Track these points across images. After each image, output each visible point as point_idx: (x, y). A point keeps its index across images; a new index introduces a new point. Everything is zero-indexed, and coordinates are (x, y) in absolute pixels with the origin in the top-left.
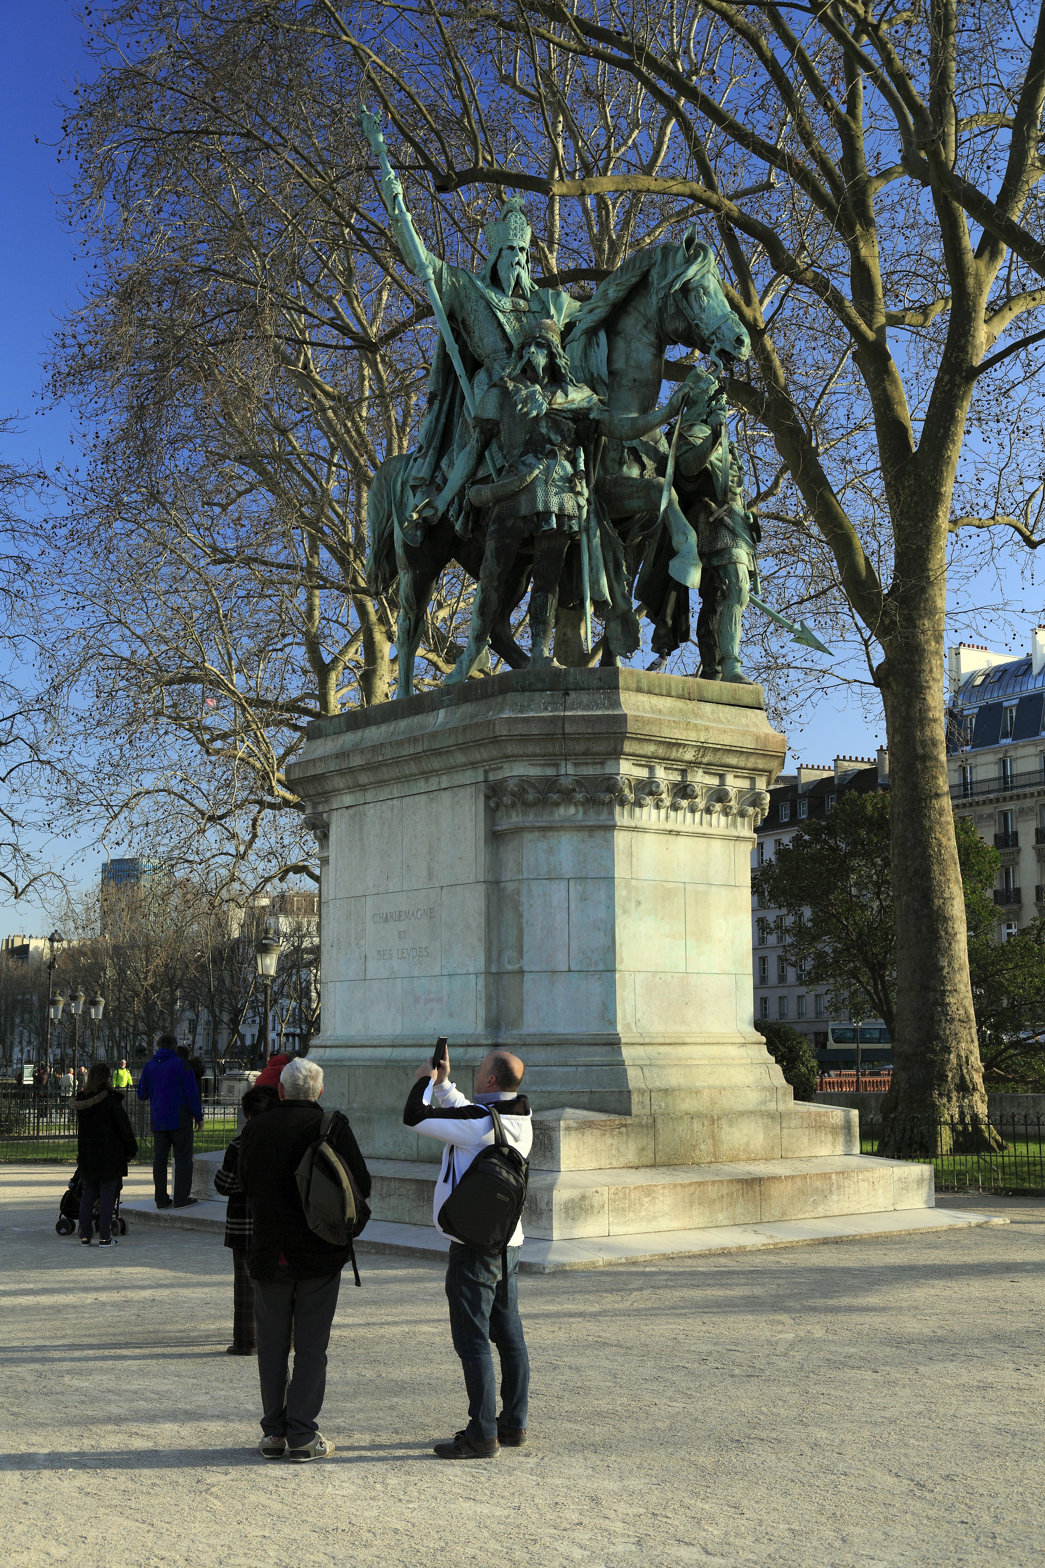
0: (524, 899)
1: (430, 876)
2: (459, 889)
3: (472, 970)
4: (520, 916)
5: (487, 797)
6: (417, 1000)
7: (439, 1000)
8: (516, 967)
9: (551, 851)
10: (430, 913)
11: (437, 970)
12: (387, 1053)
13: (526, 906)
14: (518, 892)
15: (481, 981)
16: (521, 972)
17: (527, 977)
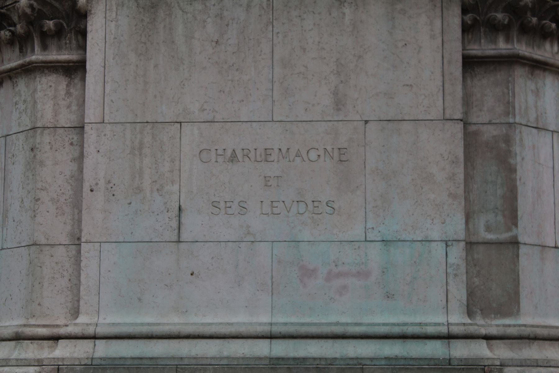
0: (517, 149)
1: (339, 104)
2: (406, 126)
3: (435, 235)
4: (512, 170)
5: (465, 11)
6: (307, 273)
7: (363, 274)
8: (504, 236)
9: (537, 93)
10: (342, 156)
11: (357, 232)
12: (262, 349)
13: (519, 159)
14: (508, 140)
15: (457, 254)
16: (515, 243)
17: (523, 250)
